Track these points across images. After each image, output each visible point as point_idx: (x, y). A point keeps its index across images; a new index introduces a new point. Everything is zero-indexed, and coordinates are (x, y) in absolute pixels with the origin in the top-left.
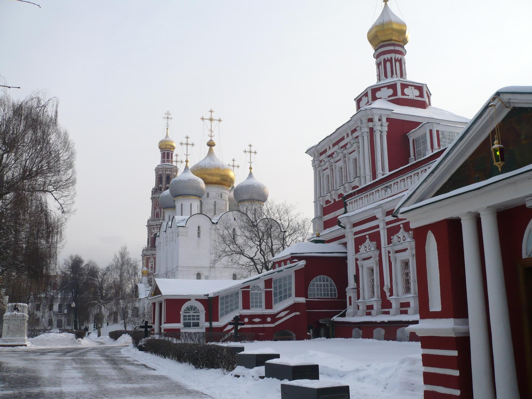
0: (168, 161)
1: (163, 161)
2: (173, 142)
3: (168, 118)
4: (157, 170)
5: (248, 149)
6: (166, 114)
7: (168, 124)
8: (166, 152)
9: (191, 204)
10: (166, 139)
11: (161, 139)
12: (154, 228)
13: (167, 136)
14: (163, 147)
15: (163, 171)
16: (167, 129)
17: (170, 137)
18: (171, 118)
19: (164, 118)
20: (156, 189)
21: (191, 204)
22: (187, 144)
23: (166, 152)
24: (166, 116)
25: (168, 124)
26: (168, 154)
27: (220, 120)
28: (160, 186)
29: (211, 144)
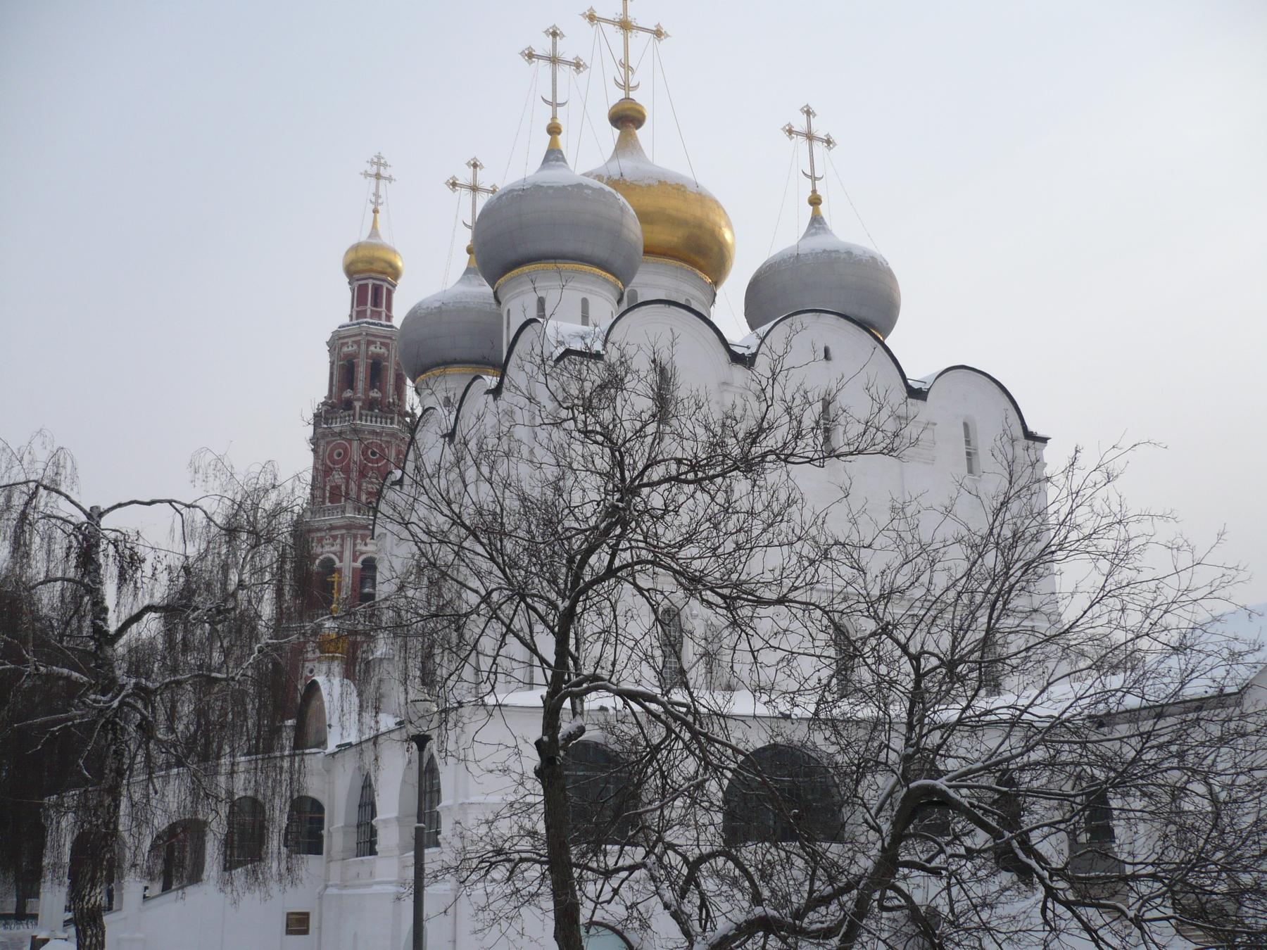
0: (379, 315)
1: (361, 314)
2: (395, 252)
3: (378, 176)
4: (336, 343)
5: (800, 124)
6: (372, 163)
7: (377, 195)
8: (370, 282)
9: (585, 302)
10: (374, 241)
11: (353, 241)
12: (320, 540)
13: (374, 231)
14: (360, 266)
15: (358, 343)
16: (375, 211)
17: (385, 238)
18: (390, 179)
19: (366, 175)
20: (333, 406)
21: (585, 302)
22: (554, 60)
23: (370, 282)
24: (373, 170)
25: (377, 195)
26: (377, 290)
27: (658, 33)
28: (348, 394)
29: (626, 118)
